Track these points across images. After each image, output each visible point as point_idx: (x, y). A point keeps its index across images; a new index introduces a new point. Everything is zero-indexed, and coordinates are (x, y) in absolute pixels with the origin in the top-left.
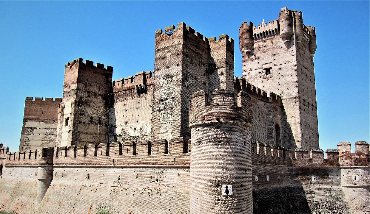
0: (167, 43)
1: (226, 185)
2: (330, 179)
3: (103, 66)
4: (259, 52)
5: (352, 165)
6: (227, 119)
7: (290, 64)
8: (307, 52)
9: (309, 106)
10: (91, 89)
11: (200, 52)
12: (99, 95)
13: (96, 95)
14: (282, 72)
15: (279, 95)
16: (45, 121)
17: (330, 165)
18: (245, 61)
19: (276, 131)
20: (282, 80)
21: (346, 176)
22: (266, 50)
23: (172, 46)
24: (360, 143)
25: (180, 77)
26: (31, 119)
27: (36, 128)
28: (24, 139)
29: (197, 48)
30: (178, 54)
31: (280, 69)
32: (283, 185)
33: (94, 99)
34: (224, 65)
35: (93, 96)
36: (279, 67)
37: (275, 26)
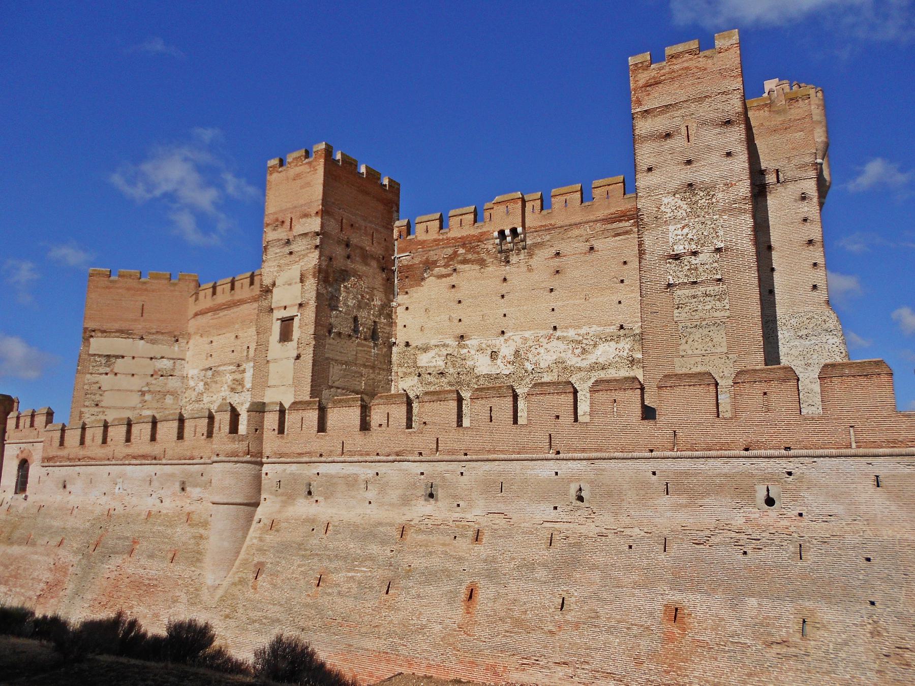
12: (373, 257)
16: (151, 337)
27: (123, 357)
28: (86, 387)
30: (728, 123)
33: (361, 268)
35: (357, 259)
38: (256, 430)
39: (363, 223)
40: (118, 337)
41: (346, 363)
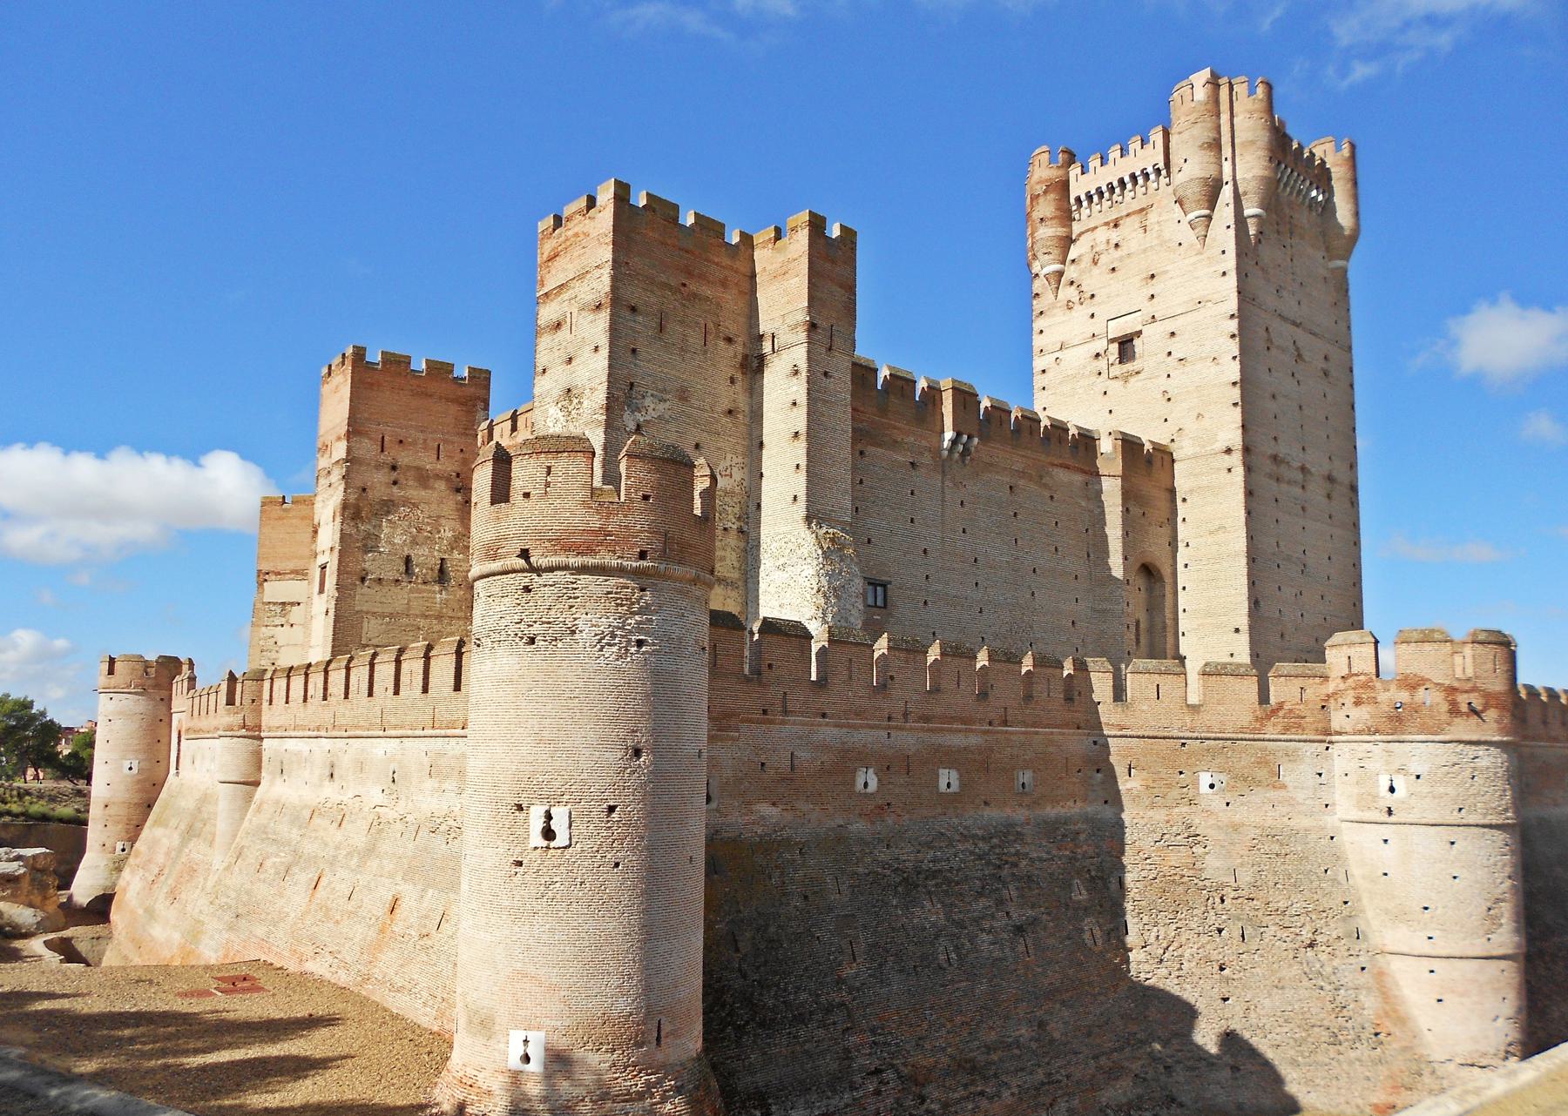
0: (570, 266)
1: (547, 808)
2: (1284, 787)
3: (449, 368)
4: (1096, 271)
5: (1376, 732)
6: (555, 553)
7: (1209, 311)
8: (1310, 251)
9: (1305, 481)
10: (405, 458)
11: (707, 291)
12: (438, 477)
13: (424, 479)
15: (1164, 441)
17: (1286, 729)
18: (1041, 313)
19: (1150, 590)
20: (1182, 379)
21: (1352, 778)
22: (1121, 259)
23: (581, 277)
24: (1415, 636)
25: (601, 396)
26: (279, 574)
27: (299, 604)
28: (261, 643)
29: (690, 274)
30: (599, 307)
31: (1173, 334)
32: (1051, 812)
33: (415, 493)
34: (803, 336)
35: (411, 483)
36: (1170, 326)
37: (1150, 156)
38: (253, 701)
39: (422, 436)
40: (293, 579)
41: (391, 616)
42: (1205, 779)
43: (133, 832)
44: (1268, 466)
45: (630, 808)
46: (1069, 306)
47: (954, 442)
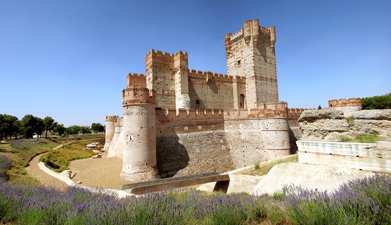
11: (167, 63)
14: (246, 62)
20: (247, 67)
37: (240, 34)
42: (241, 125)
43: (111, 139)
44: (260, 78)
45: (141, 135)
46: (231, 57)
47: (209, 80)
